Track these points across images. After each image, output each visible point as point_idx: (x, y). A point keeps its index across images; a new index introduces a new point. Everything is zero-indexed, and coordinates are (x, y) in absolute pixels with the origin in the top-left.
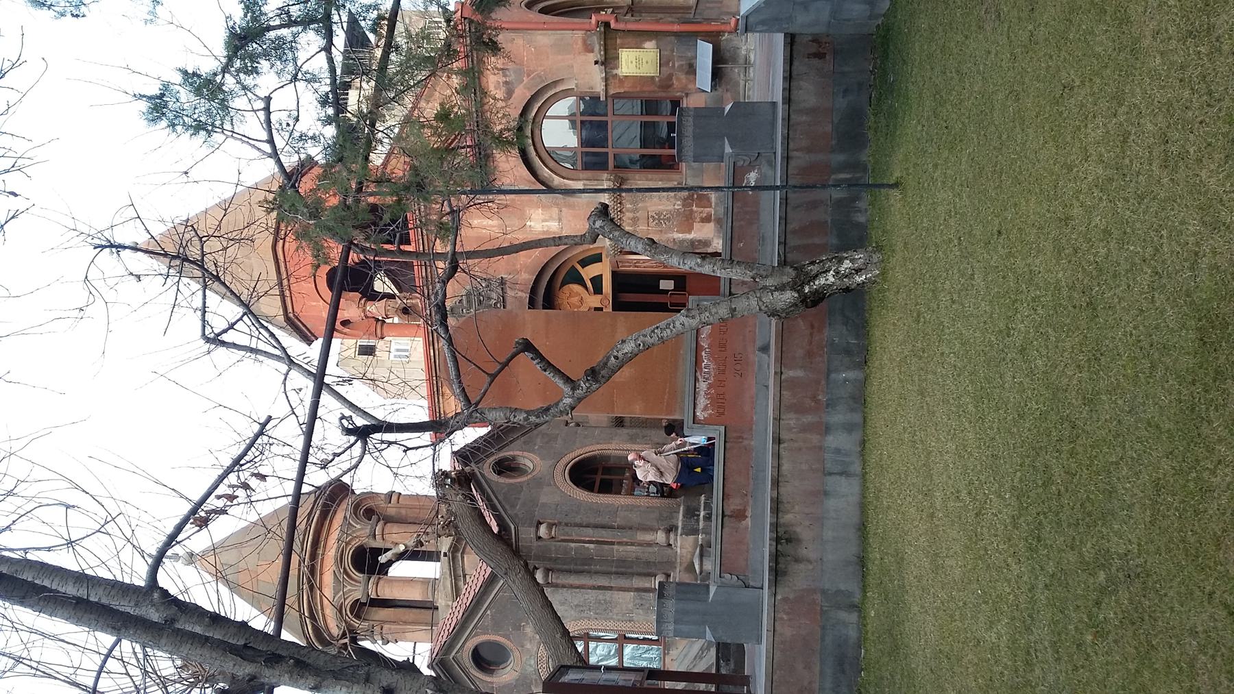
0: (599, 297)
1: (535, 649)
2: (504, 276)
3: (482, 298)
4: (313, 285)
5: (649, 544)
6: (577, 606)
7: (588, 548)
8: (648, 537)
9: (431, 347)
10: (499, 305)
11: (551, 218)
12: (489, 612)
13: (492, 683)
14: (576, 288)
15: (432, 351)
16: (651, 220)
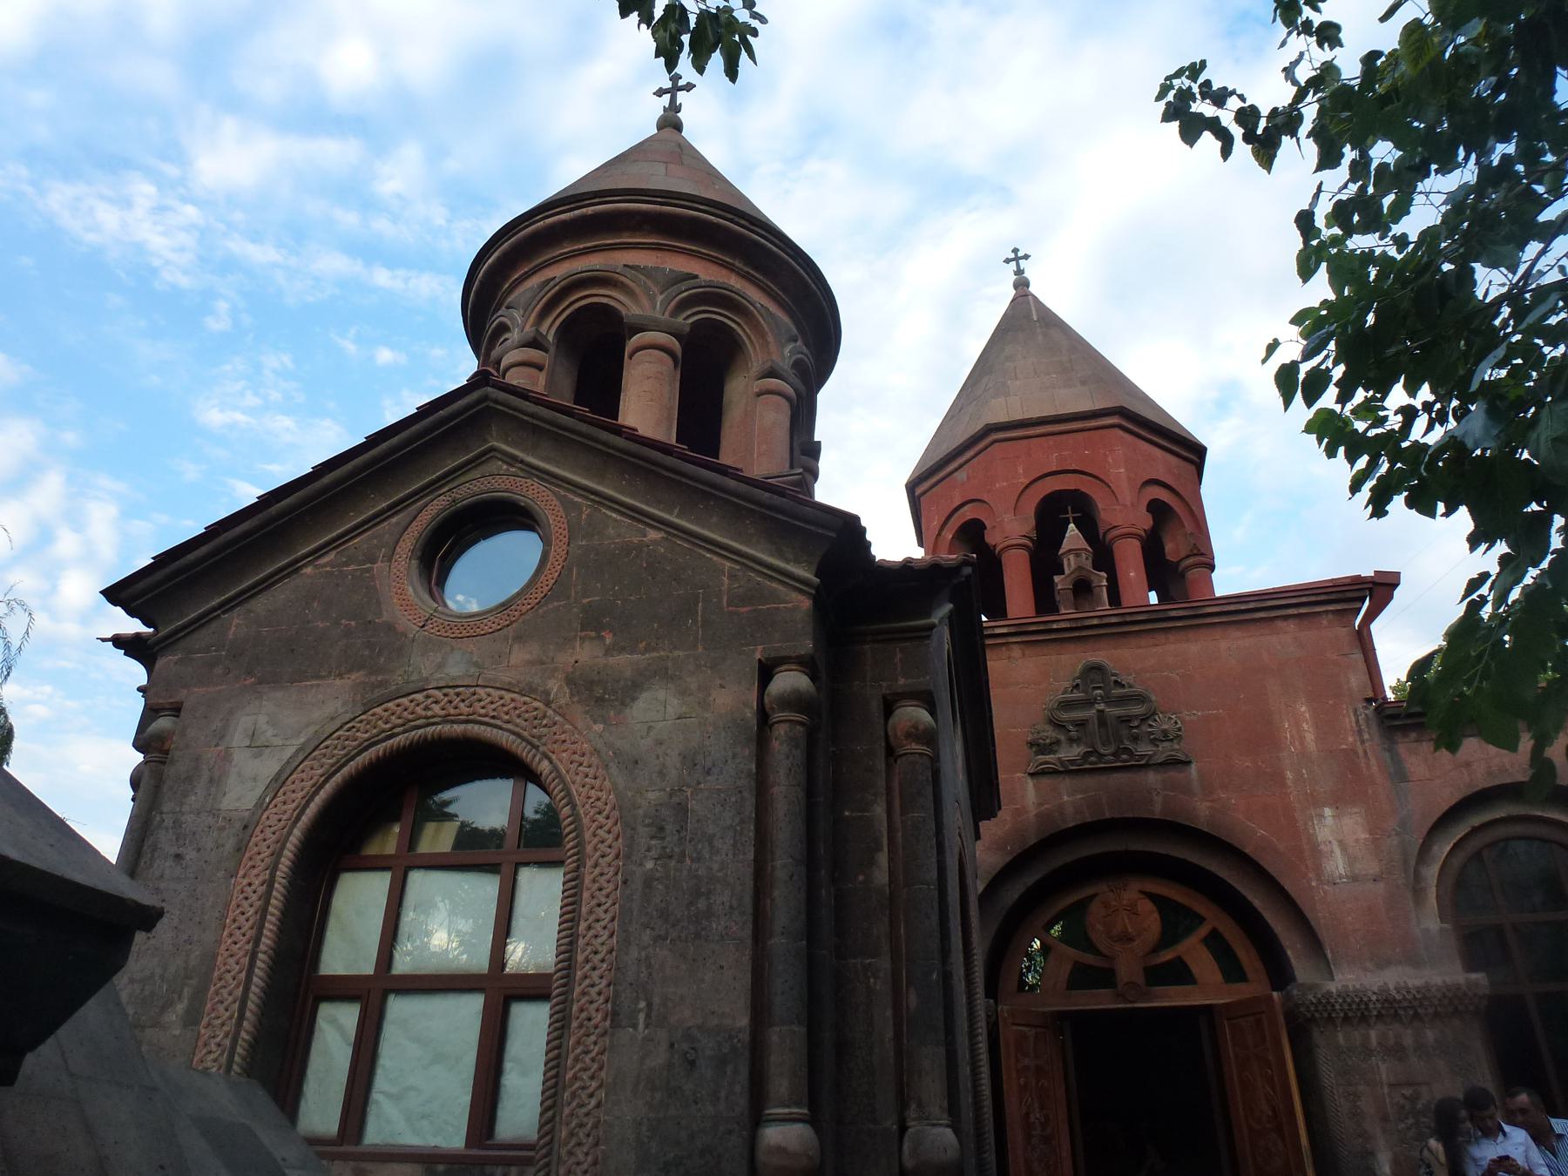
1: (506, 677)
2: (1193, 766)
3: (1136, 723)
4: (1055, 469)
5: (903, 1098)
6: (682, 810)
8: (931, 1087)
9: (1012, 630)
10: (1124, 756)
11: (1351, 860)
12: (653, 535)
13: (389, 558)
14: (1151, 922)
15: (1005, 630)
16: (1408, 1092)
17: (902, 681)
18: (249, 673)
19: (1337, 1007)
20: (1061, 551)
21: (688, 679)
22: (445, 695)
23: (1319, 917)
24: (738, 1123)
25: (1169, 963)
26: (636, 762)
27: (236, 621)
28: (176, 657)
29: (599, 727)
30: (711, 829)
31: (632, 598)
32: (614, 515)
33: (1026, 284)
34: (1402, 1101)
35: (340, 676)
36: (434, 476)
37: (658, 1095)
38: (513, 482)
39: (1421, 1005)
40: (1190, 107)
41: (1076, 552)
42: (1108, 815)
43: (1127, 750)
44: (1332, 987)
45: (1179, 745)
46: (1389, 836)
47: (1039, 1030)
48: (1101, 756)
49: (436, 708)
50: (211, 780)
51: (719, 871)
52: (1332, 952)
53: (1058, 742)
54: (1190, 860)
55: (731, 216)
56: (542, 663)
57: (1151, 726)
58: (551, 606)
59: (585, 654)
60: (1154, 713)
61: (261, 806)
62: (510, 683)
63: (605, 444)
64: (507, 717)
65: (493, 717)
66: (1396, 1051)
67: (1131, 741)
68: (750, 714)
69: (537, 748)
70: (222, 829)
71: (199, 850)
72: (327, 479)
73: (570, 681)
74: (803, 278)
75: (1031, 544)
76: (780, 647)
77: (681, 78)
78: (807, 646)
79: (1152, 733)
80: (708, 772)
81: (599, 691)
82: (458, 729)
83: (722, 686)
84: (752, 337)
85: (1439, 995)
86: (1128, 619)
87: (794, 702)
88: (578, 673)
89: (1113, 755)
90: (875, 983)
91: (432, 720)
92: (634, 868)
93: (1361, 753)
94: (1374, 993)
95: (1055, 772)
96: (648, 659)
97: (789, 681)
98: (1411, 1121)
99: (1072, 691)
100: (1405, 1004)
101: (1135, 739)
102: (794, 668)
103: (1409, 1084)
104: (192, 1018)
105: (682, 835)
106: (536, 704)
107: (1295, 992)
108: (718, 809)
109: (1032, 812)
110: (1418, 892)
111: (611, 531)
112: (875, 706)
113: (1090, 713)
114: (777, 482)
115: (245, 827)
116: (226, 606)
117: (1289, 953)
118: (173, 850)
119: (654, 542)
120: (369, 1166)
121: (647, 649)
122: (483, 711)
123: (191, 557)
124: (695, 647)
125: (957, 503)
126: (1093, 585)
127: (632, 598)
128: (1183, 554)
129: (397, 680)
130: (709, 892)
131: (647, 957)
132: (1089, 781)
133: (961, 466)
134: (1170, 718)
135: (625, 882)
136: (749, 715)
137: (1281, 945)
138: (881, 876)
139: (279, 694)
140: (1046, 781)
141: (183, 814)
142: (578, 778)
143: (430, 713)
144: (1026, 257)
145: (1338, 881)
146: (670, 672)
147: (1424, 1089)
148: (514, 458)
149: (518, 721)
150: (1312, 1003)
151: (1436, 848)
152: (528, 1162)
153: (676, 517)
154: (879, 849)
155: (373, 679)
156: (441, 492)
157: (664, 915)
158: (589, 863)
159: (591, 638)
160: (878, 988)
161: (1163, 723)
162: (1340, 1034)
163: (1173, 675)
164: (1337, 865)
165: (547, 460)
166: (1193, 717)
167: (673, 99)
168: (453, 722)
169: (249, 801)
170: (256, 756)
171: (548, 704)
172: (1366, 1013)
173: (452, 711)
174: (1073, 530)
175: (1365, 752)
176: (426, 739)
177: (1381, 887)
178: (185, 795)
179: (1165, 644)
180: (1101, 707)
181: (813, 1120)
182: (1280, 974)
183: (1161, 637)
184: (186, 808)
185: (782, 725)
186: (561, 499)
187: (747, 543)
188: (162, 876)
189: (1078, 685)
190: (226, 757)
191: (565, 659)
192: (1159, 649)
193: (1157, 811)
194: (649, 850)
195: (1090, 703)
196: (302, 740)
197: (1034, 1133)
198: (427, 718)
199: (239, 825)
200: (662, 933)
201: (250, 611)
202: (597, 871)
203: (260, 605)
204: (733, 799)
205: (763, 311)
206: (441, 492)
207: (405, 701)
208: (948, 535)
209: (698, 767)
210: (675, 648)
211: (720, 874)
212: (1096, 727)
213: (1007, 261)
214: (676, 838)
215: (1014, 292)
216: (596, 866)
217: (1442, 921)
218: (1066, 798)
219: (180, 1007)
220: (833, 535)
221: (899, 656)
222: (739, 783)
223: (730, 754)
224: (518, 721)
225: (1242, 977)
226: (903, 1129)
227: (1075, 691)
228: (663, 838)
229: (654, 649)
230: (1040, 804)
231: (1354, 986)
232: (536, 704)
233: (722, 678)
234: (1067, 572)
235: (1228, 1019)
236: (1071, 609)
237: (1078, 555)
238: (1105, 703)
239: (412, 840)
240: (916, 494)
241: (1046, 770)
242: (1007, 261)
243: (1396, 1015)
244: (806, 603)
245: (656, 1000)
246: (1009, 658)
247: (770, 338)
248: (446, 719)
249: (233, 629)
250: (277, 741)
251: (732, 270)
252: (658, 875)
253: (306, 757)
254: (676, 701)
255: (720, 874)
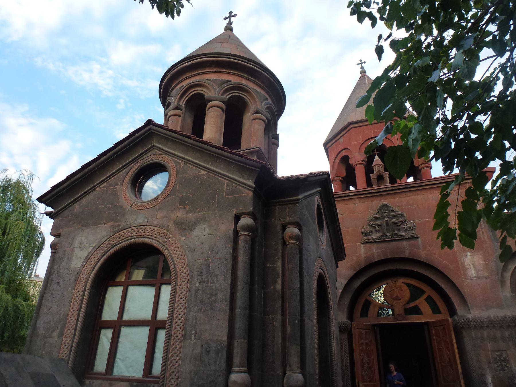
0: (402, 312)
1: (155, 222)
2: (420, 239)
3: (399, 224)
5: (285, 363)
6: (208, 266)
7: (276, 282)
8: (294, 360)
10: (395, 236)
11: (477, 271)
12: (203, 172)
14: (407, 293)
16: (498, 353)
17: (288, 219)
18: (80, 223)
19: (472, 323)
20: (373, 165)
21: (212, 222)
22: (137, 229)
23: (466, 291)
24: (222, 373)
25: (413, 307)
26: (195, 250)
27: (77, 207)
28: (59, 219)
29: (183, 238)
30: (217, 273)
31: (195, 194)
32: (191, 166)
33: (365, 72)
34: (496, 357)
35: (106, 223)
36: (136, 156)
37: (197, 362)
38: (160, 157)
39: (503, 323)
40: (361, 9)
41: (378, 165)
42: (389, 257)
43: (396, 234)
44: (470, 316)
45: (414, 231)
46: (491, 262)
47: (367, 330)
48: (387, 236)
49: (134, 233)
50: (68, 259)
51: (219, 287)
52: (470, 303)
53: (372, 232)
54: (419, 271)
55: (241, 59)
56: (167, 217)
57: (405, 225)
58: (170, 198)
59: (180, 214)
60: (406, 221)
61: (82, 266)
62: (156, 224)
63: (186, 142)
64: (155, 236)
65: (151, 236)
66: (494, 339)
67: (398, 231)
68: (231, 233)
69: (164, 246)
70: (71, 274)
71: (64, 281)
72: (102, 159)
73: (175, 223)
74: (270, 79)
75: (365, 163)
76: (242, 209)
77: (232, 13)
78: (250, 209)
79: (405, 228)
80: (217, 253)
81: (184, 226)
82: (141, 240)
83: (223, 223)
84: (251, 100)
85: (510, 319)
86: (396, 188)
87: (247, 228)
88: (177, 220)
89: (391, 236)
90: (276, 324)
91: (133, 237)
92: (192, 286)
93: (481, 233)
94: (485, 318)
95: (371, 242)
96: (199, 215)
97: (246, 221)
98: (499, 364)
99: (377, 214)
100: (497, 322)
101: (399, 230)
102: (246, 216)
103: (499, 351)
104: (61, 335)
105: (208, 274)
106: (164, 231)
107: (456, 318)
108: (220, 266)
109: (363, 256)
110: (502, 282)
111: (190, 172)
112: (279, 228)
113: (383, 222)
114: (243, 153)
115: (78, 273)
116: (74, 202)
117: (455, 304)
118: (57, 281)
119: (203, 175)
120: (113, 382)
121: (200, 211)
122: (148, 234)
123: (62, 187)
124: (215, 210)
125: (340, 150)
126: (384, 177)
127: (195, 194)
128: (420, 164)
129: (123, 224)
130: (216, 294)
131: (196, 316)
132: (383, 245)
133: (341, 137)
134: (412, 222)
135: (189, 291)
136: (231, 233)
137: (452, 301)
138: (279, 287)
139: (88, 230)
140: (367, 245)
141: (60, 269)
142: (176, 256)
143: (132, 235)
144: (365, 62)
145: (472, 278)
146: (206, 219)
147: (504, 352)
148: (160, 148)
149: (158, 237)
150: (462, 322)
151: (510, 266)
152: (157, 382)
153: (210, 165)
154: (279, 277)
155: (116, 224)
156: (138, 161)
157: (201, 302)
158: (179, 284)
159: (182, 208)
160: (277, 325)
161: (409, 224)
162: (473, 333)
163: (413, 207)
164: (472, 273)
165: (170, 148)
166: (420, 222)
167: (230, 20)
168: (139, 238)
169: (79, 265)
170: (81, 250)
171: (168, 231)
172: (483, 326)
173: (139, 234)
174: (377, 158)
175: (483, 232)
176: (131, 243)
177: (488, 280)
178: (61, 263)
179: (409, 196)
180: (387, 219)
181: (249, 372)
182: (452, 312)
183: (408, 194)
184: (61, 267)
185: (242, 236)
186: (175, 162)
187: (232, 174)
188: (53, 289)
189: (379, 212)
190: (73, 251)
191: (174, 215)
192: (408, 198)
193: (407, 255)
194: (197, 280)
195: (382, 218)
196: (95, 245)
197: (365, 366)
198: (132, 236)
199: (76, 273)
200: (201, 308)
201: (81, 203)
202: (181, 287)
203: (84, 201)
204: (225, 262)
205: (254, 91)
206: (138, 161)
207: (125, 231)
208: (337, 161)
209: (214, 251)
210: (208, 211)
211: (219, 288)
212: (385, 226)
213: (358, 64)
214: (206, 275)
215: (360, 75)
216: (181, 285)
217: (512, 293)
218: (375, 251)
219: (58, 331)
220: (259, 170)
221: (287, 210)
222: (227, 257)
223: (224, 246)
224: (158, 237)
225: (439, 312)
226: (285, 374)
227: (378, 214)
228: (202, 276)
229: (201, 212)
230: (366, 254)
231: (478, 316)
232: (164, 231)
233: (222, 221)
234: (375, 172)
235: (434, 327)
236: (376, 185)
237: (378, 167)
238: (388, 218)
239: (129, 277)
240: (327, 147)
241: (368, 242)
242: (358, 64)
243: (494, 326)
244: (251, 194)
245: (198, 331)
246: (355, 203)
247: (257, 100)
248: (137, 237)
249: (76, 209)
250: (87, 245)
251: (243, 78)
252: (200, 288)
253: (96, 250)
254: (208, 229)
255: (219, 288)
